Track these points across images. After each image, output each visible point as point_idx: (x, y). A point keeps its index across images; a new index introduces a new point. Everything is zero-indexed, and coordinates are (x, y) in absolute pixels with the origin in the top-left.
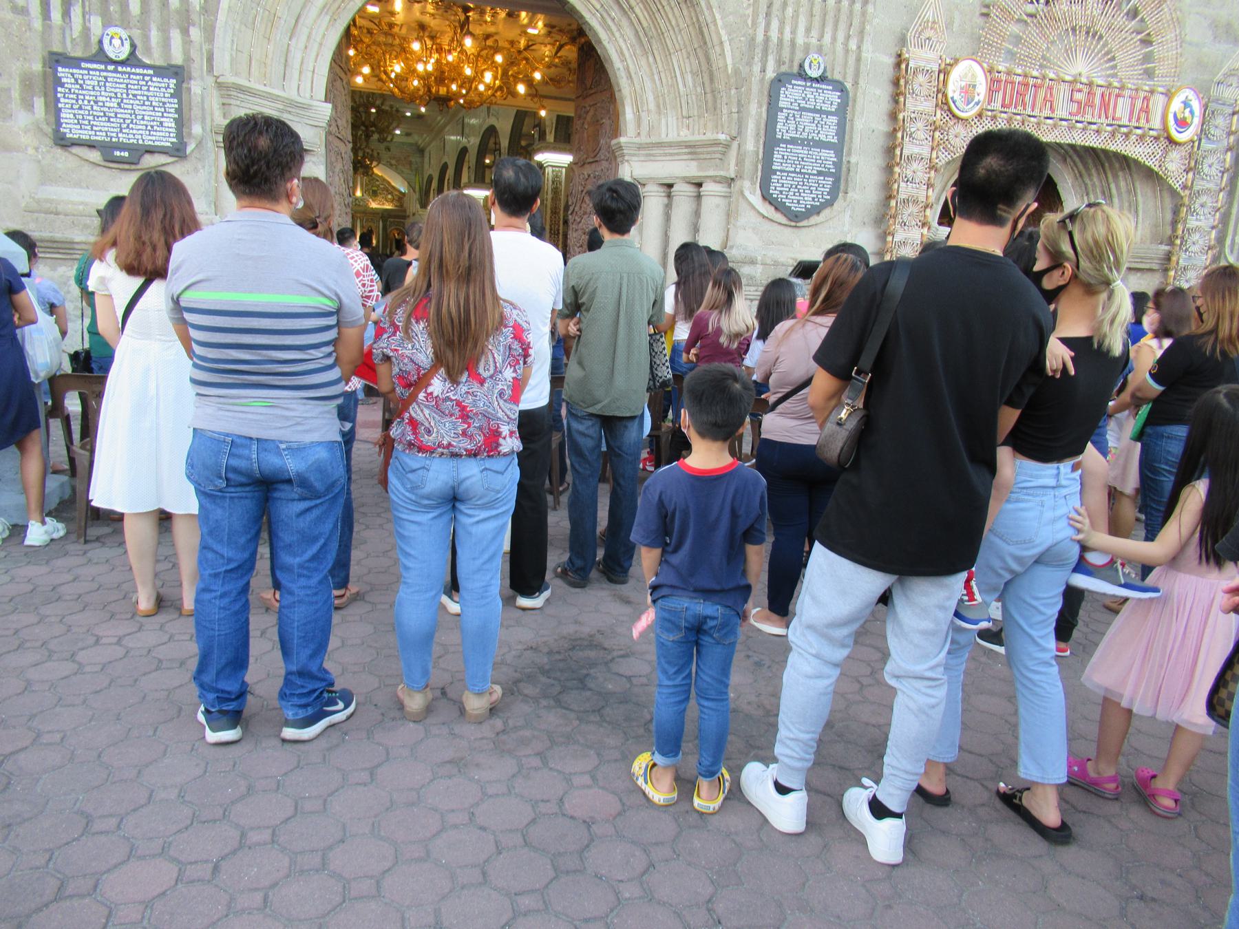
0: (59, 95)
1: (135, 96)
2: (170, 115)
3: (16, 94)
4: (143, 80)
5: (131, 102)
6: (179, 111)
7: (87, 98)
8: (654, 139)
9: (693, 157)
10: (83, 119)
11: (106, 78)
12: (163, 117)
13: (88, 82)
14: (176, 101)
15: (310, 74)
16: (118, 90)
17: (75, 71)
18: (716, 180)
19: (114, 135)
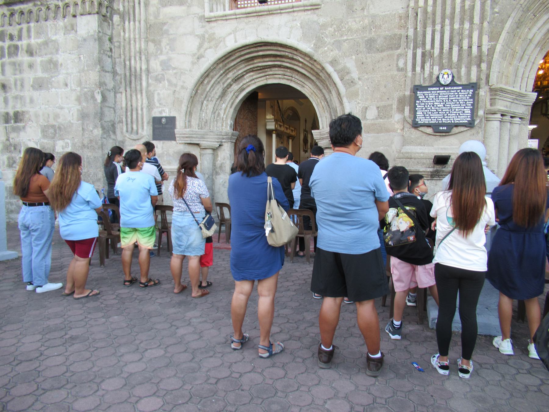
0: (417, 104)
1: (451, 100)
2: (469, 107)
3: (395, 107)
4: (457, 92)
5: (450, 103)
6: (473, 105)
7: (429, 104)
10: (427, 114)
11: (439, 93)
12: (465, 108)
13: (430, 97)
14: (472, 100)
15: (526, 79)
16: (444, 98)
17: (425, 92)
19: (440, 120)
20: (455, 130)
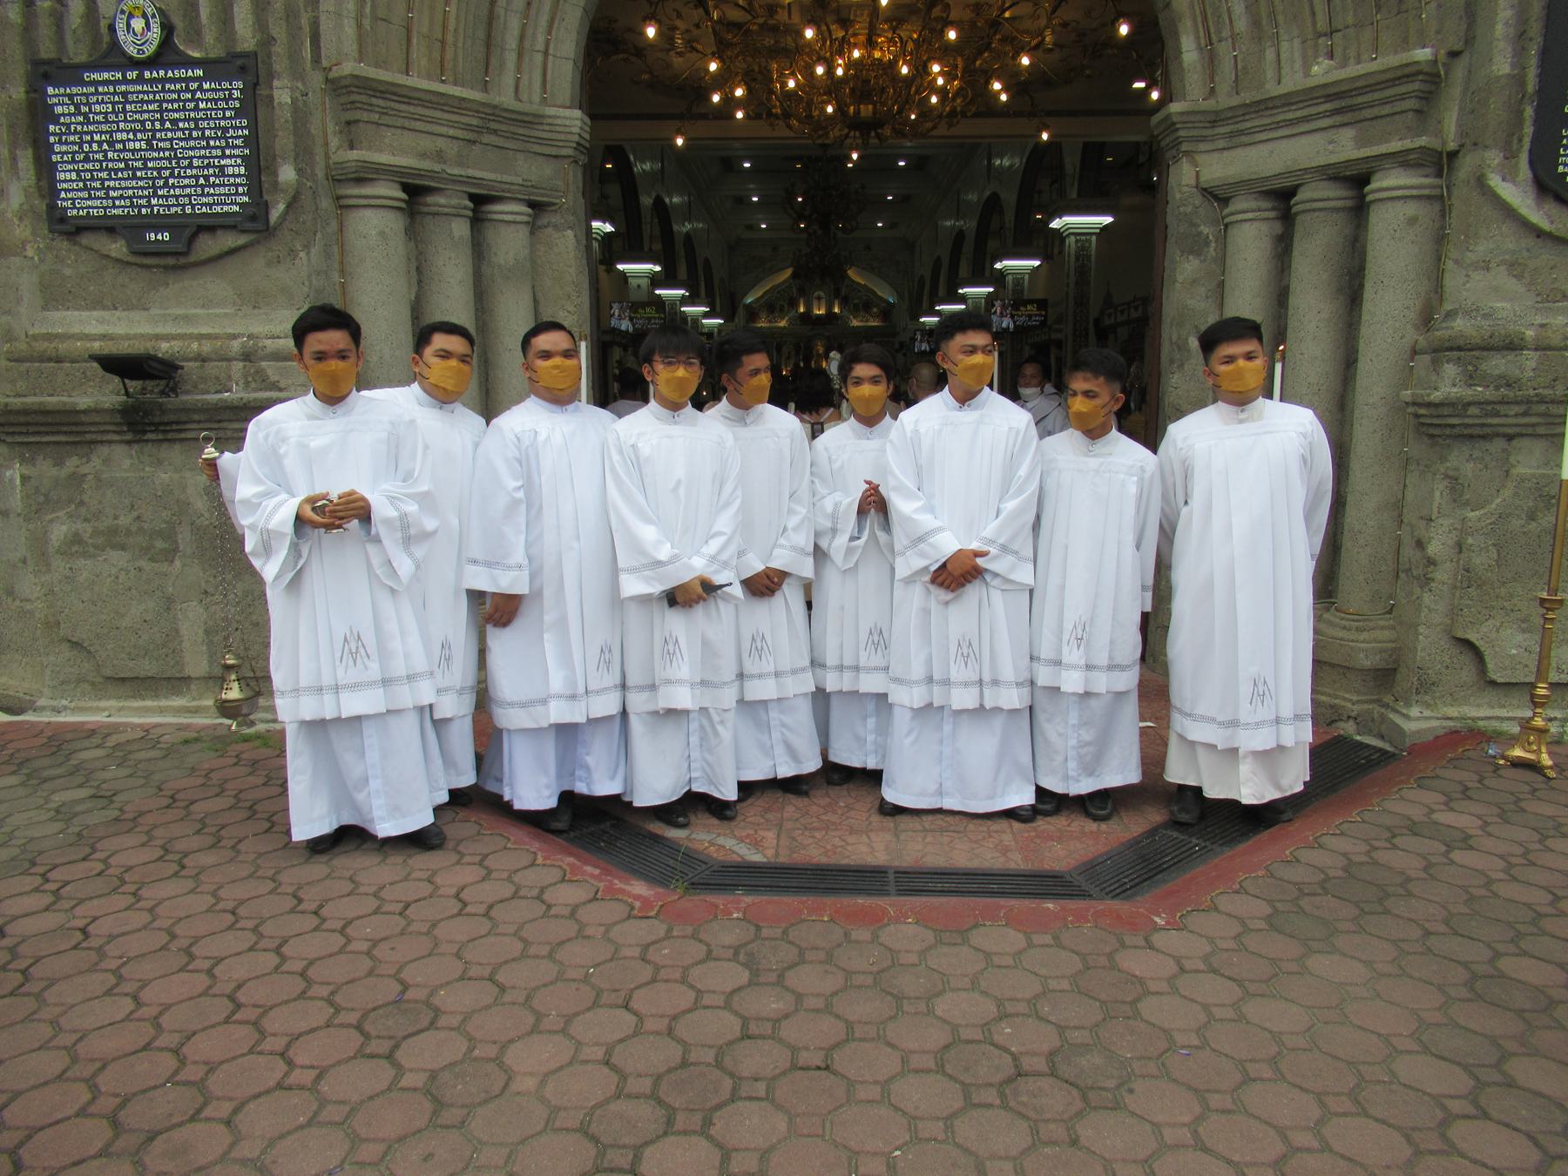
0: (52, 139)
1: (174, 122)
2: (236, 152)
4: (187, 90)
5: (169, 135)
6: (252, 141)
7: (97, 138)
8: (1247, 97)
9: (1338, 119)
10: (92, 179)
11: (125, 94)
12: (224, 156)
13: (97, 108)
14: (245, 122)
15: (539, 58)
16: (146, 116)
17: (75, 90)
18: (1402, 160)
19: (143, 202)
20: (208, 245)
